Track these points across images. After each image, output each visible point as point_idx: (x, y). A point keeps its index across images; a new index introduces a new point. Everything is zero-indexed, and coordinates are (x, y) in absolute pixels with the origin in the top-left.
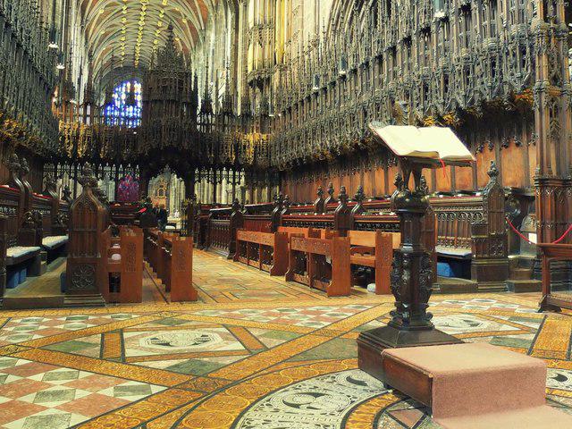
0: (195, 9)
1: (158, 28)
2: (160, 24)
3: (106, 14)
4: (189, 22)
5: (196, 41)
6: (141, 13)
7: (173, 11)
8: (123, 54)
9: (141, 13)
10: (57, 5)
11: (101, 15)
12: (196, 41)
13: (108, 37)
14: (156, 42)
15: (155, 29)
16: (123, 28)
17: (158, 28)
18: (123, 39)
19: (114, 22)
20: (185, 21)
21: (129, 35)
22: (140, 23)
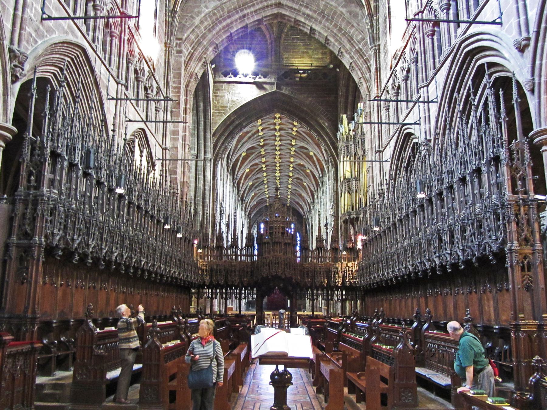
0: (314, 162)
1: (290, 177)
3: (251, 171)
4: (311, 171)
5: (318, 185)
6: (277, 168)
7: (299, 165)
8: (267, 196)
9: (277, 168)
10: (206, 178)
11: (247, 172)
13: (254, 186)
14: (290, 186)
15: (287, 178)
16: (265, 179)
17: (290, 177)
18: (266, 186)
19: (258, 176)
20: (308, 171)
21: (270, 184)
22: (276, 175)
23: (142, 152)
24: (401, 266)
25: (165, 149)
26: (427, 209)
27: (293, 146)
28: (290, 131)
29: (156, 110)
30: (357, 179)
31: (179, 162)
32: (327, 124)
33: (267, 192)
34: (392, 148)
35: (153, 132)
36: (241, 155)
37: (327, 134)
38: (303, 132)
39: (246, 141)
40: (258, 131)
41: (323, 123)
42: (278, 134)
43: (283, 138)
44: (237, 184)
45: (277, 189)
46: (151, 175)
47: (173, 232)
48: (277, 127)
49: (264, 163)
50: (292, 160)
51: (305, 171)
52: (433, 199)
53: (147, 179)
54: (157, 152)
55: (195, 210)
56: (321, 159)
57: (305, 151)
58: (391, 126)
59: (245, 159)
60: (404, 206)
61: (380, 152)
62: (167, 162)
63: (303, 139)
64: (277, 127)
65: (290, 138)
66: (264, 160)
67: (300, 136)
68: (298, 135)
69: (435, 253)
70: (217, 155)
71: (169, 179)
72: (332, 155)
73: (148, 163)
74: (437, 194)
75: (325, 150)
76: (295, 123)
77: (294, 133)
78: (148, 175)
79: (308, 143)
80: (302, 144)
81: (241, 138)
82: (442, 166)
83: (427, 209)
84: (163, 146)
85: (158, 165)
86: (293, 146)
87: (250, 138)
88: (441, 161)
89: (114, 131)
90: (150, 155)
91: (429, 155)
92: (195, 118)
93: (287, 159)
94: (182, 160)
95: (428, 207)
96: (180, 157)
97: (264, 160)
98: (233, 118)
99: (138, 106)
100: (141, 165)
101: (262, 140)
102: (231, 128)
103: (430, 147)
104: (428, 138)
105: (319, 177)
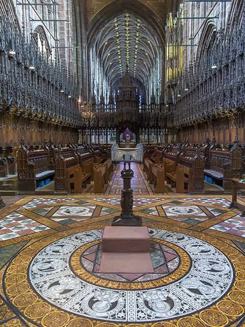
0: (150, 48)
1: (136, 59)
2: (136, 57)
3: (111, 55)
7: (141, 50)
12: (152, 64)
14: (135, 65)
17: (136, 59)
21: (123, 64)
23: (42, 42)
24: (200, 113)
25: (57, 40)
26: (218, 76)
27: (137, 37)
28: (135, 26)
29: (49, 12)
30: (177, 58)
31: (66, 49)
32: (159, 20)
33: (121, 70)
34: (200, 36)
35: (48, 28)
36: (104, 44)
37: (159, 27)
38: (145, 27)
39: (108, 34)
40: (115, 27)
41: (157, 20)
42: (127, 28)
43: (131, 31)
44: (102, 64)
45: (127, 66)
46: (50, 58)
47: (66, 95)
48: (127, 24)
49: (119, 49)
50: (137, 47)
51: (145, 54)
52: (223, 70)
53: (48, 61)
54: (52, 42)
55: (78, 82)
56: (155, 45)
57: (145, 40)
58: (200, 19)
59: (107, 46)
60: (204, 75)
61: (192, 39)
62: (59, 49)
63: (144, 32)
64: (127, 24)
65: (135, 31)
66: (119, 47)
67: (142, 29)
68: (140, 28)
69: (221, 104)
70: (89, 44)
71: (60, 61)
72: (162, 43)
73: (47, 50)
74: (225, 66)
75: (157, 39)
76: (139, 21)
77: (138, 28)
78: (47, 58)
79: (147, 34)
80: (143, 35)
81: (105, 31)
82: (229, 47)
83: (218, 76)
84: (55, 38)
85: (53, 50)
86: (137, 37)
87: (110, 31)
88: (229, 44)
89: (23, 27)
90: (48, 45)
91: (222, 40)
92: (74, 18)
93: (134, 46)
94: (67, 47)
95: (219, 75)
96: (66, 46)
97: (119, 47)
98: (98, 17)
99: (36, 10)
100: (43, 51)
101: (117, 33)
102: (97, 25)
103: (224, 34)
104: (223, 28)
105: (154, 58)
